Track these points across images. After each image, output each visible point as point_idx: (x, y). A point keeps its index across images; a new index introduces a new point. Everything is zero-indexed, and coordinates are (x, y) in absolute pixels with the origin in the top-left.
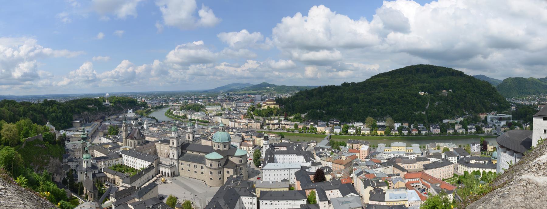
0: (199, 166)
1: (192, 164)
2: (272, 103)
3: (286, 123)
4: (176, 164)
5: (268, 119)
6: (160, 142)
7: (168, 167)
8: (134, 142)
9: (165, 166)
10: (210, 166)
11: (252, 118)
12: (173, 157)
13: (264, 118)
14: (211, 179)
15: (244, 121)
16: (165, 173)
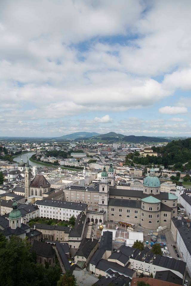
0: (132, 210)
1: (125, 209)
2: (150, 151)
3: (167, 171)
4: (106, 210)
5: (148, 167)
6: (70, 189)
7: (101, 213)
8: (41, 190)
9: (97, 213)
10: (150, 210)
11: (132, 165)
12: (103, 202)
13: (145, 166)
14: (150, 222)
15: (124, 168)
16: (96, 220)
